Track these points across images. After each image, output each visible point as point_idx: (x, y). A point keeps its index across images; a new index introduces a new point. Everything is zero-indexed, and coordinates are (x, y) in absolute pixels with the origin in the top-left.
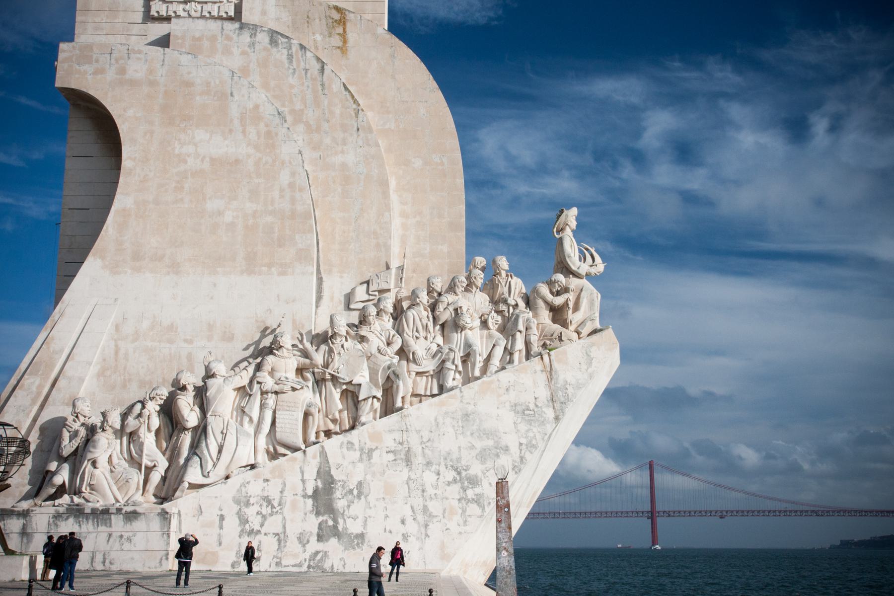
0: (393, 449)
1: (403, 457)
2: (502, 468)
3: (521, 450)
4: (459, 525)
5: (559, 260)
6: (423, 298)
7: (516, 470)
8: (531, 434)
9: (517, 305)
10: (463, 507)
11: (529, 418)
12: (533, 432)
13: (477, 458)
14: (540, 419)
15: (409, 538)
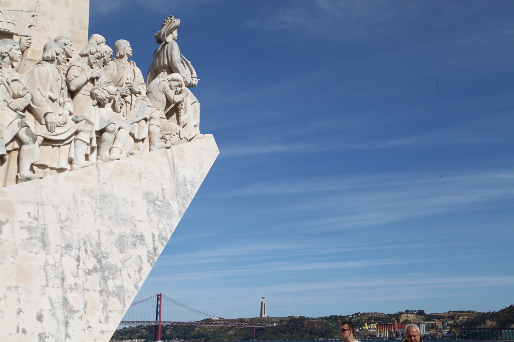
0: (27, 225)
1: (39, 235)
2: (139, 258)
3: (154, 241)
4: (100, 322)
5: (166, 63)
6: (62, 57)
7: (151, 261)
8: (161, 226)
9: (140, 93)
10: (104, 300)
11: (159, 209)
12: (163, 224)
13: (116, 246)
14: (167, 211)
15: (47, 340)
